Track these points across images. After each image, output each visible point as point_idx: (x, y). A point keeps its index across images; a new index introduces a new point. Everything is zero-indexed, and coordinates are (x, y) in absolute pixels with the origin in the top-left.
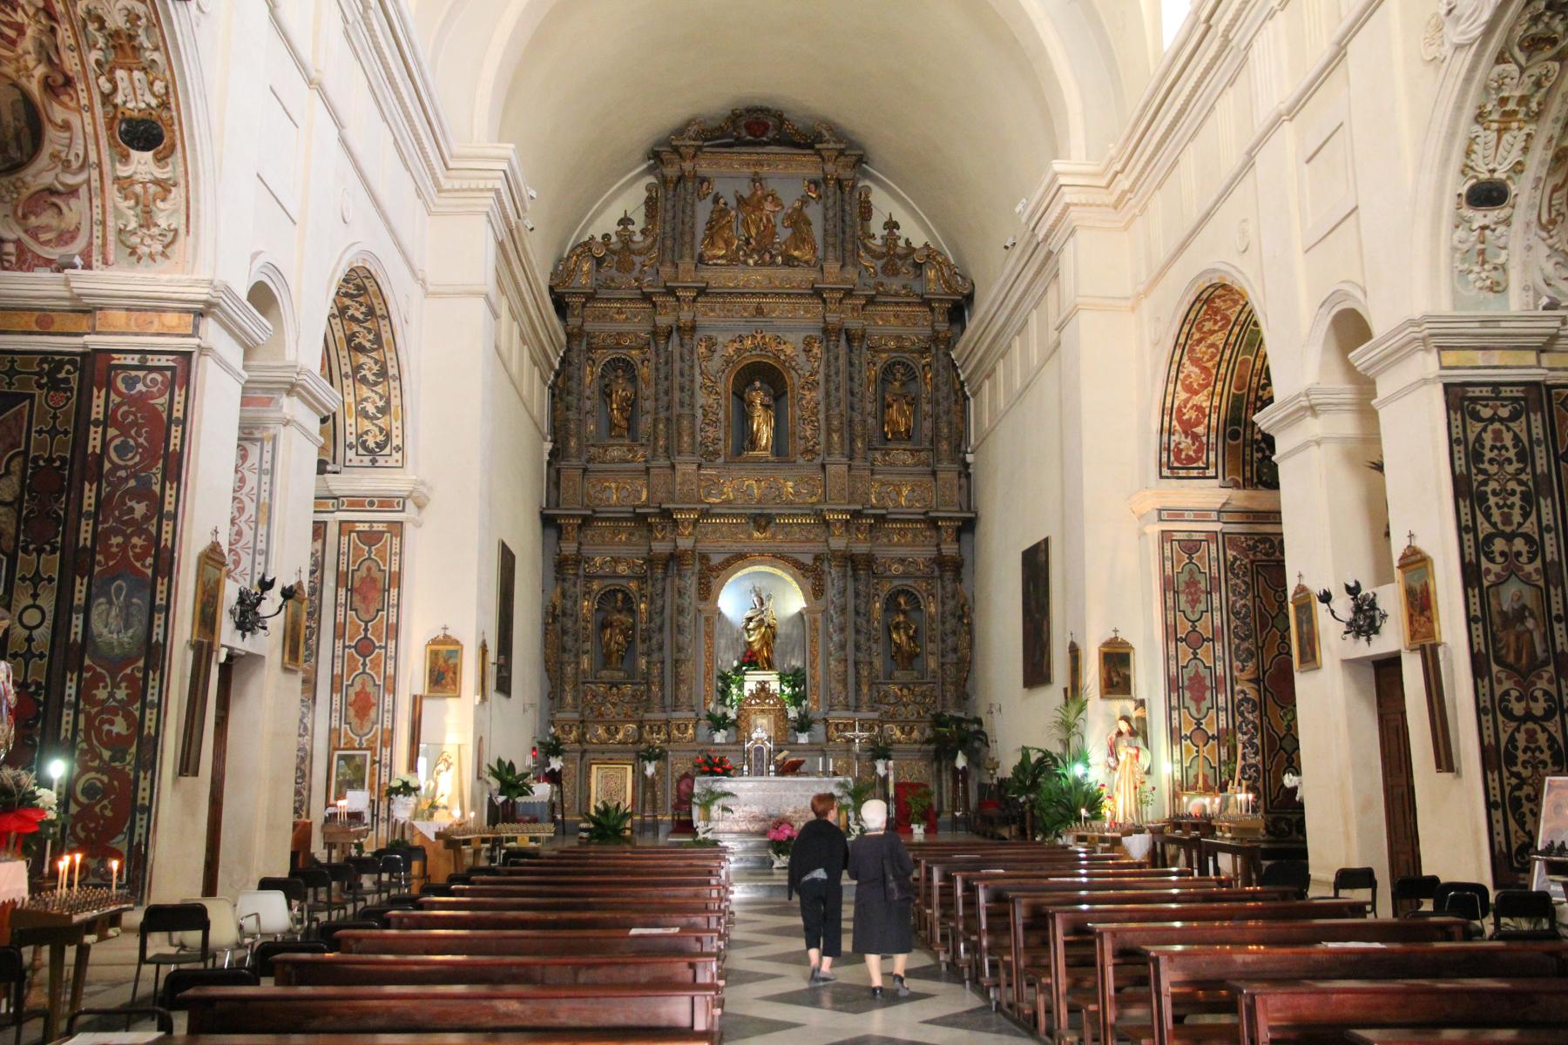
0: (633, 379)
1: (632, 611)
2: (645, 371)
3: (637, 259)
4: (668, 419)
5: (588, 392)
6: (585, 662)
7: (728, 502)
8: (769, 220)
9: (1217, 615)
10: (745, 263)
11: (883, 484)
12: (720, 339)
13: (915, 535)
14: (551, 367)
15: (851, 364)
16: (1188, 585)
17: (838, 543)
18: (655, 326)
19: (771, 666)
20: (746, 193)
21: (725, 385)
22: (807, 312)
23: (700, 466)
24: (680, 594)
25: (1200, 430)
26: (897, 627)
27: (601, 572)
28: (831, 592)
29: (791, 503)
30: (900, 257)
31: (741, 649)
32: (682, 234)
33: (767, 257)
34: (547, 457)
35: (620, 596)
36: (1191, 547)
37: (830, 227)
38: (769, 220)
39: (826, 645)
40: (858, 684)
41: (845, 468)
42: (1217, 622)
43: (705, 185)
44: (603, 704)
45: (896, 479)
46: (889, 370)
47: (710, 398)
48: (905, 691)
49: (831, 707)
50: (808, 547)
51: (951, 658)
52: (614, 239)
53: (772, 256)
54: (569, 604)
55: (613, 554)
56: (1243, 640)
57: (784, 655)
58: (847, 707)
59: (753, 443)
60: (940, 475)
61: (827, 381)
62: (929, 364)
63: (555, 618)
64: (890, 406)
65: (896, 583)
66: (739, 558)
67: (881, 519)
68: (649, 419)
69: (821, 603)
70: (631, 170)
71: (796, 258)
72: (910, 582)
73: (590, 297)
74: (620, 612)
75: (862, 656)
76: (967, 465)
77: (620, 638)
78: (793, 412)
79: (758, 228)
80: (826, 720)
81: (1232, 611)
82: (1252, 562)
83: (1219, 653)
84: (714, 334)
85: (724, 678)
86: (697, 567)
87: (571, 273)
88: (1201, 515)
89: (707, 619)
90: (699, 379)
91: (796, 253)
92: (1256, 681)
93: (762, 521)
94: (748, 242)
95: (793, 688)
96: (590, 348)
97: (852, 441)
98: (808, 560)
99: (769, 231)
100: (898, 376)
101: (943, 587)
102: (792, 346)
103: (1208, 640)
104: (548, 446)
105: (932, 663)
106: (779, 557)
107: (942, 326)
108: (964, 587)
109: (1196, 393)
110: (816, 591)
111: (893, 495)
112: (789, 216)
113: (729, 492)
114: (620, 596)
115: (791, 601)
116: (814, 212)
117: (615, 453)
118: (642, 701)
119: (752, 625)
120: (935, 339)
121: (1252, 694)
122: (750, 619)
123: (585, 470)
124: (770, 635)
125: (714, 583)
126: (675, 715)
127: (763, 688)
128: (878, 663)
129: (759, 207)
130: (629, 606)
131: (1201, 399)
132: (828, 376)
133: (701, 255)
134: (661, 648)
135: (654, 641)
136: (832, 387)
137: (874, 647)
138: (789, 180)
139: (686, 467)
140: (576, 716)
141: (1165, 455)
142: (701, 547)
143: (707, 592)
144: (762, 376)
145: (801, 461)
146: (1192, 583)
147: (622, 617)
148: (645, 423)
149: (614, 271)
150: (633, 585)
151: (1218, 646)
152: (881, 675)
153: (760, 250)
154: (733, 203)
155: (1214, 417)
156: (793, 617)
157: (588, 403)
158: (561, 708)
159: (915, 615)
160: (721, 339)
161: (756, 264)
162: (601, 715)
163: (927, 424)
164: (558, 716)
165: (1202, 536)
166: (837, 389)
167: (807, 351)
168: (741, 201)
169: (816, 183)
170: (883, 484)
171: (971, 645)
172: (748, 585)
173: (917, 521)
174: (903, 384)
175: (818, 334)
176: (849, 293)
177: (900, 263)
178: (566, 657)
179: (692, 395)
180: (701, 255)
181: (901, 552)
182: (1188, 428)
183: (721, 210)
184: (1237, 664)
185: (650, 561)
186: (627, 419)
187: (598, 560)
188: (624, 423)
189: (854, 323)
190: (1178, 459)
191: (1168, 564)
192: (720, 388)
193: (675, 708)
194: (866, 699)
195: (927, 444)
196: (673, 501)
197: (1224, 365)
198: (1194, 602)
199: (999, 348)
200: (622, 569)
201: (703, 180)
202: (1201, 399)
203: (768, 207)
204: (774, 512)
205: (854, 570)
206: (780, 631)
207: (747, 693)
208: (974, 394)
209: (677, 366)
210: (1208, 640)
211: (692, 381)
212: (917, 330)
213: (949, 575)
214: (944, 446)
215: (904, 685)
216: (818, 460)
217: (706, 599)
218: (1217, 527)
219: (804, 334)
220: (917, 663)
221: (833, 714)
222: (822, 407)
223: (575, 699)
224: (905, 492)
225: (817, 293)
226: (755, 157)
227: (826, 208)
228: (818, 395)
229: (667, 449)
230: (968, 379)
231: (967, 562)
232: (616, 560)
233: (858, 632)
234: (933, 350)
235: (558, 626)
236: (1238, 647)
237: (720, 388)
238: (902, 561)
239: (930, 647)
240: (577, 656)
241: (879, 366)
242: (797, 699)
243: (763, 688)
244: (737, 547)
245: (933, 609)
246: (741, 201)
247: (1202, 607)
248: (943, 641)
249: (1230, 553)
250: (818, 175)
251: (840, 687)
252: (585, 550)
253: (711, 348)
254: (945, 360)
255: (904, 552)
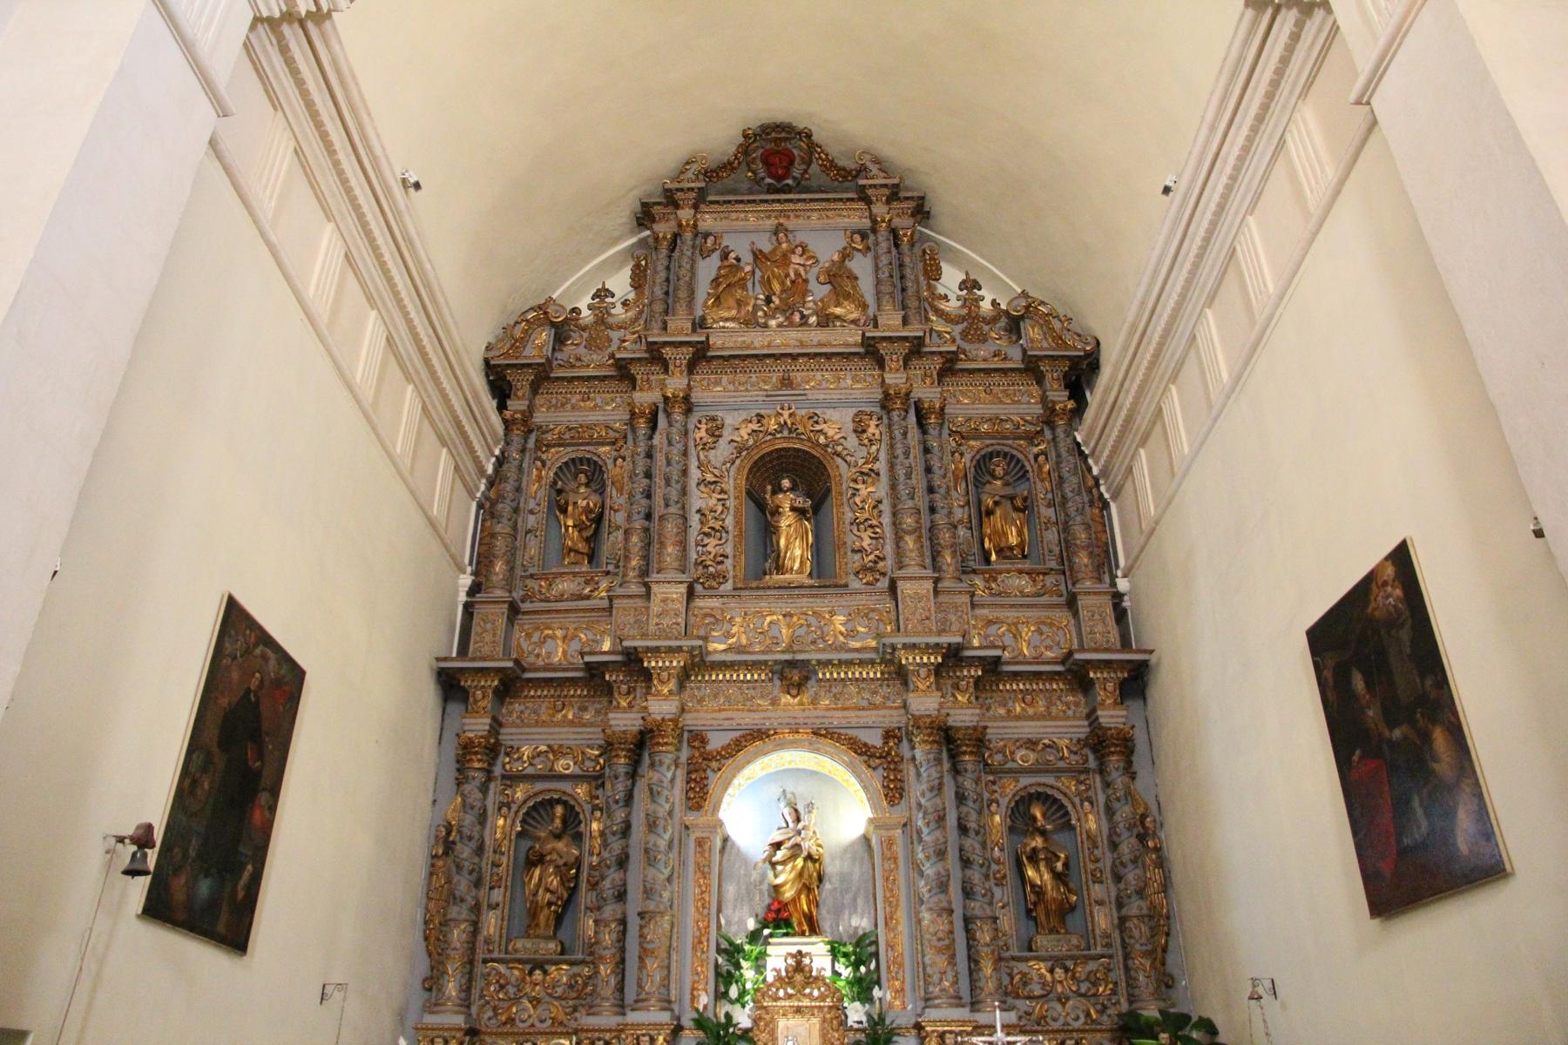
0: (601, 491)
1: (578, 838)
2: (613, 471)
3: (615, 335)
4: (646, 530)
5: (532, 504)
6: (491, 923)
7: (740, 649)
8: (798, 274)
10: (766, 326)
11: (990, 622)
12: (729, 421)
13: (1050, 704)
14: (481, 471)
15: (927, 451)
17: (925, 702)
18: (631, 405)
19: (814, 929)
20: (767, 247)
21: (734, 482)
22: (855, 380)
23: (691, 594)
24: (653, 794)
26: (1033, 857)
27: (530, 771)
28: (917, 789)
29: (843, 648)
30: (986, 321)
31: (762, 902)
32: (676, 289)
33: (797, 317)
34: (463, 597)
35: (559, 810)
37: (884, 275)
38: (798, 274)
39: (911, 885)
40: (973, 960)
41: (929, 585)
43: (710, 240)
44: (516, 1000)
45: (1011, 615)
46: (983, 464)
47: (712, 495)
48: (1059, 972)
49: (928, 1000)
50: (870, 717)
51: (1135, 907)
52: (585, 313)
53: (803, 316)
54: (469, 819)
55: (551, 738)
57: (837, 912)
58: (957, 1001)
59: (780, 568)
60: (1083, 602)
61: (892, 466)
62: (1043, 453)
63: (449, 847)
64: (990, 513)
65: (1025, 781)
66: (756, 738)
67: (992, 667)
68: (620, 535)
69: (899, 814)
70: (616, 241)
71: (838, 317)
72: (1050, 780)
73: (542, 376)
74: (558, 837)
75: (976, 907)
76: (1118, 597)
77: (554, 882)
78: (841, 513)
79: (782, 284)
80: (918, 1027)
84: (720, 414)
85: (732, 952)
86: (685, 754)
87: (518, 344)
89: (700, 843)
90: (695, 474)
91: (838, 311)
93: (794, 674)
94: (768, 301)
95: (856, 966)
96: (539, 445)
97: (935, 556)
98: (874, 739)
99: (799, 287)
100: (999, 471)
101: (1107, 785)
102: (836, 424)
104: (466, 580)
105: (1103, 920)
106: (824, 735)
107: (1060, 396)
108: (1140, 785)
110: (894, 791)
111: (1008, 640)
112: (828, 272)
113: (739, 633)
114: (559, 810)
115: (846, 811)
116: (861, 266)
117: (565, 586)
118: (581, 996)
119: (780, 855)
120: (1049, 417)
122: (777, 846)
123: (514, 610)
124: (813, 878)
125: (713, 779)
126: (633, 1017)
127: (799, 965)
128: (1006, 922)
129: (785, 260)
130: (572, 825)
132: (892, 458)
133: (703, 319)
134: (621, 896)
135: (607, 884)
136: (901, 472)
137: (998, 892)
138: (823, 234)
139: (669, 592)
140: (459, 1020)
142: (689, 720)
143: (699, 794)
144: (792, 471)
145: (855, 584)
147: (560, 845)
148: (612, 542)
149: (582, 351)
150: (581, 791)
152: (1013, 942)
153: (787, 309)
154: (747, 258)
156: (853, 844)
157: (532, 520)
158: (433, 1006)
159: (1061, 838)
160: (730, 420)
161: (780, 325)
162: (511, 1020)
163: (1051, 536)
164: (430, 1019)
166: (908, 476)
167: (860, 431)
168: (758, 256)
169: (864, 236)
170: (990, 622)
171: (1166, 887)
172: (777, 791)
173: (1052, 676)
174: (1007, 484)
175: (878, 409)
176: (916, 349)
177: (986, 328)
178: (454, 912)
179: (684, 492)
180: (703, 319)
181: (1029, 729)
183: (731, 266)
185: (608, 748)
186: (587, 540)
187: (526, 751)
188: (582, 546)
189: (927, 393)
192: (729, 484)
193: (640, 1003)
194: (991, 986)
195: (1053, 564)
196: (644, 636)
199: (1144, 427)
200: (564, 765)
201: (706, 235)
203: (796, 259)
204: (814, 657)
205: (954, 756)
206: (831, 868)
207: (770, 977)
208: (1115, 497)
209: (660, 458)
211: (685, 472)
212: (1022, 408)
213: (1114, 761)
214: (1083, 559)
215: (1056, 962)
216: (884, 583)
217: (699, 807)
219: (855, 410)
220: (1074, 920)
221: (932, 1014)
222: (886, 507)
223: (467, 989)
224: (1027, 632)
225: (871, 352)
226: (777, 207)
227: (876, 258)
228: (881, 489)
229: (644, 572)
230: (1105, 472)
231: (1140, 737)
232: (556, 751)
233: (966, 863)
234: (1048, 434)
235: (450, 860)
237: (729, 484)
238: (1031, 744)
239: (1097, 891)
240: (476, 908)
241: (968, 457)
242: (863, 989)
243: (799, 965)
244: (749, 720)
245: (1092, 825)
246: (758, 256)
248: (1118, 878)
250: (866, 223)
251: (942, 961)
252: (508, 736)
253: (715, 432)
254: (1069, 441)
255: (1035, 727)
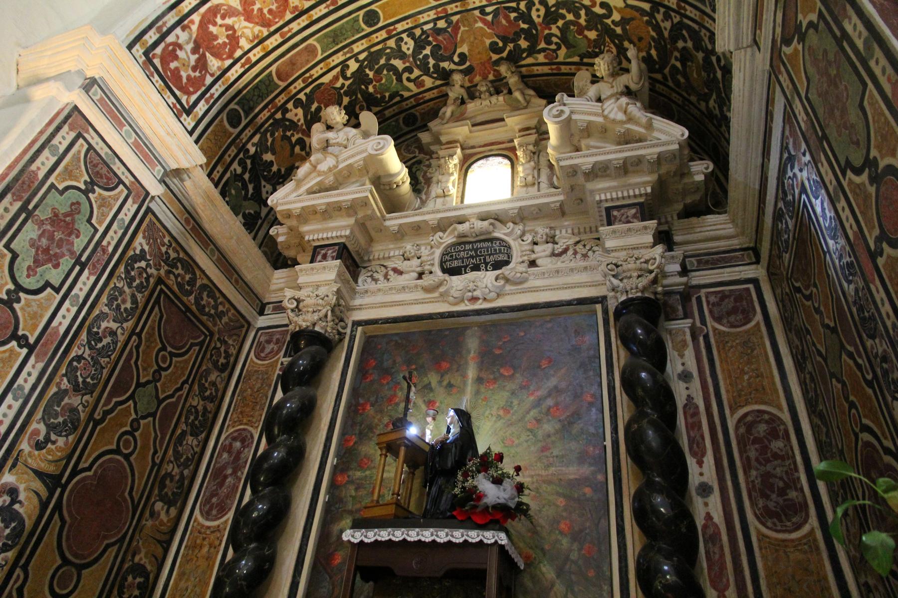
9: (68, 312)
16: (56, 219)
25: (214, 64)
36: (102, 173)
42: (62, 322)
56: (76, 388)
81: (85, 324)
82: (160, 281)
83: (26, 381)
88: (145, 149)
92: (52, 481)
103: (22, 341)
109: (249, 18)
121: (27, 507)
131: (247, 30)
141: (152, 37)
146: (64, 223)
151: (33, 368)
155: (238, 69)
165: (127, 179)
182: (204, 43)
184: (38, 426)
190: (165, 60)
191: (46, 160)
197: (303, 21)
198: (45, 255)
202: (247, 30)
210: (22, 341)
218: (155, 189)
236: (61, 395)
247: (55, 276)
249: (140, 243)
